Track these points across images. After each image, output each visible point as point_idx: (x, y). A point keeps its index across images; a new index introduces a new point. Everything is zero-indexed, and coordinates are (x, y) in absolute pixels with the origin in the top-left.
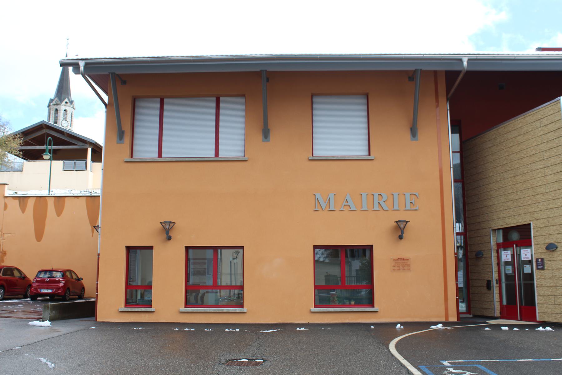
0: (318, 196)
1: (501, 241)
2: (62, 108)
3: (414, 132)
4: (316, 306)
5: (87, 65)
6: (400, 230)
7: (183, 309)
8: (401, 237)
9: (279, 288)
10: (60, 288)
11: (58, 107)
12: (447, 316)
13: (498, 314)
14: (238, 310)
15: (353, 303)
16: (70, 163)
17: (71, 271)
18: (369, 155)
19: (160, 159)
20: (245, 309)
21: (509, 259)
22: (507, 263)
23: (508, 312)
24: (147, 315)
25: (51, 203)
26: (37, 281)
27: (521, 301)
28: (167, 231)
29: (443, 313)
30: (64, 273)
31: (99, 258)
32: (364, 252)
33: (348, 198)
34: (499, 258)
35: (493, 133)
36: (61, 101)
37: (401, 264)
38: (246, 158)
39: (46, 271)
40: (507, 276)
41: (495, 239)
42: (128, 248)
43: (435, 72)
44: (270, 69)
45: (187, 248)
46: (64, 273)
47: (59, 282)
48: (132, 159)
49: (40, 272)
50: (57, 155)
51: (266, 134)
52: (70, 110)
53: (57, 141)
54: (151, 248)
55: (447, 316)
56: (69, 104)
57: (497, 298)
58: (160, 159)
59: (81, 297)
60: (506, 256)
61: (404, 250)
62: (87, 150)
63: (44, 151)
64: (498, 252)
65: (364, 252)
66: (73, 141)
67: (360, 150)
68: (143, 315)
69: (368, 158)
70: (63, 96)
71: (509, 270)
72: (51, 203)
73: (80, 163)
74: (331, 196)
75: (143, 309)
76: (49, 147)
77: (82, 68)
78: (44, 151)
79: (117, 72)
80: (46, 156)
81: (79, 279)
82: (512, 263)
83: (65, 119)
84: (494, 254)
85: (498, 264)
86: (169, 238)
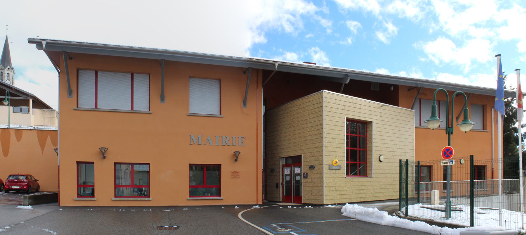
0: (192, 136)
1: (284, 164)
2: (6, 72)
3: (244, 102)
4: (190, 197)
5: (47, 44)
6: (236, 157)
7: (114, 198)
8: (236, 160)
9: (171, 187)
10: (24, 186)
11: (3, 71)
12: (257, 202)
13: (281, 200)
14: (147, 199)
15: (209, 195)
16: (18, 108)
17: (30, 176)
18: (220, 114)
19: (96, 109)
20: (150, 198)
21: (289, 172)
22: (287, 175)
23: (287, 198)
24: (92, 202)
25: (13, 134)
26: (9, 181)
27: (293, 192)
28: (103, 153)
29: (256, 200)
30: (27, 177)
31: (59, 169)
32: (218, 167)
33: (209, 138)
34: (283, 172)
35: (284, 107)
36: (5, 67)
37: (235, 174)
38: (150, 112)
39: (14, 175)
40: (287, 182)
41: (281, 163)
42: (78, 163)
43: (258, 70)
44: (166, 59)
45: (115, 164)
46: (27, 177)
47: (24, 182)
48: (78, 108)
49: (10, 176)
50: (13, 103)
51: (162, 98)
52: (11, 73)
53: (12, 95)
54: (93, 163)
55: (257, 202)
56: (10, 70)
57: (281, 192)
58: (96, 109)
59: (37, 191)
60: (287, 171)
61: (237, 167)
62: (29, 100)
63: (4, 99)
64: (283, 169)
65: (218, 167)
66: (19, 94)
67: (214, 110)
68: (89, 202)
69: (220, 115)
70: (6, 64)
71: (288, 178)
72: (13, 134)
73: (24, 109)
74: (200, 137)
75: (89, 199)
76: (7, 97)
77: (44, 46)
78: (4, 99)
79: (68, 51)
80: (6, 103)
81: (36, 181)
82: (290, 175)
83: (8, 79)
84: (281, 170)
85: (283, 175)
86: (104, 158)
